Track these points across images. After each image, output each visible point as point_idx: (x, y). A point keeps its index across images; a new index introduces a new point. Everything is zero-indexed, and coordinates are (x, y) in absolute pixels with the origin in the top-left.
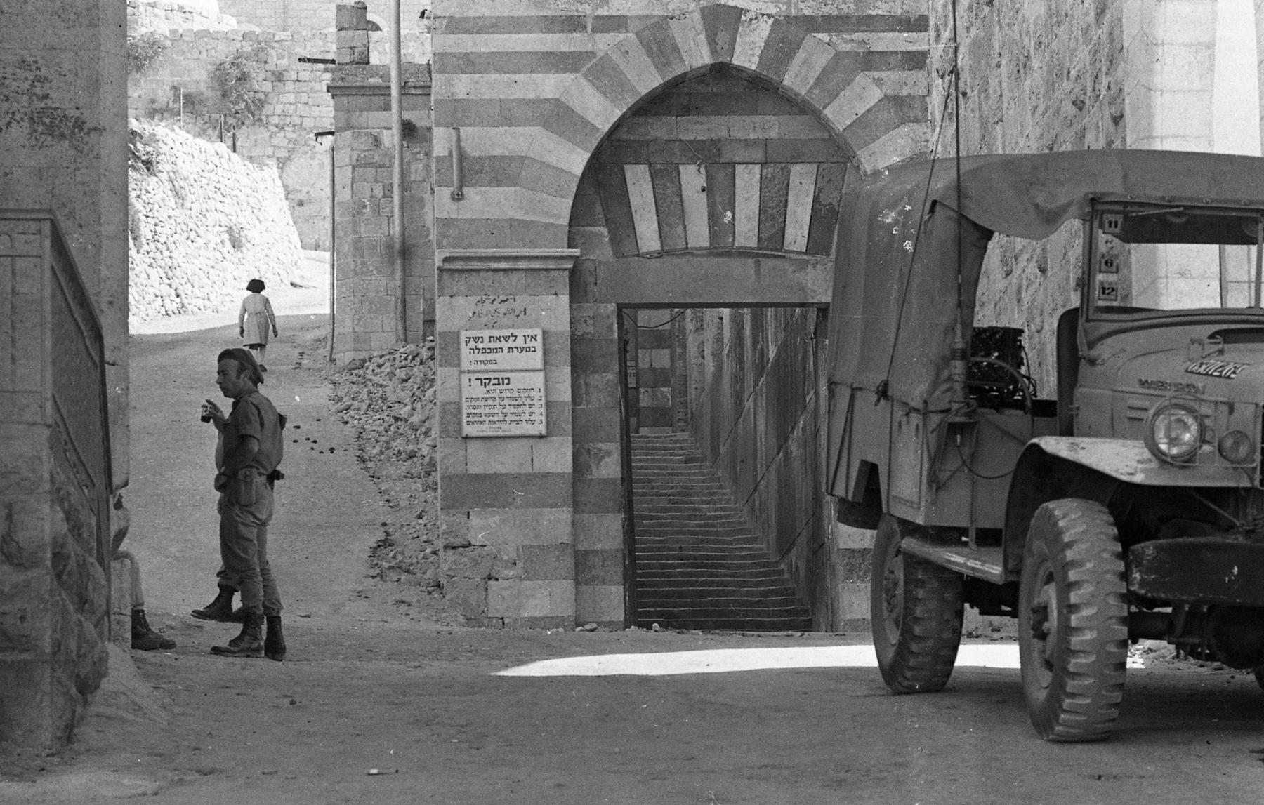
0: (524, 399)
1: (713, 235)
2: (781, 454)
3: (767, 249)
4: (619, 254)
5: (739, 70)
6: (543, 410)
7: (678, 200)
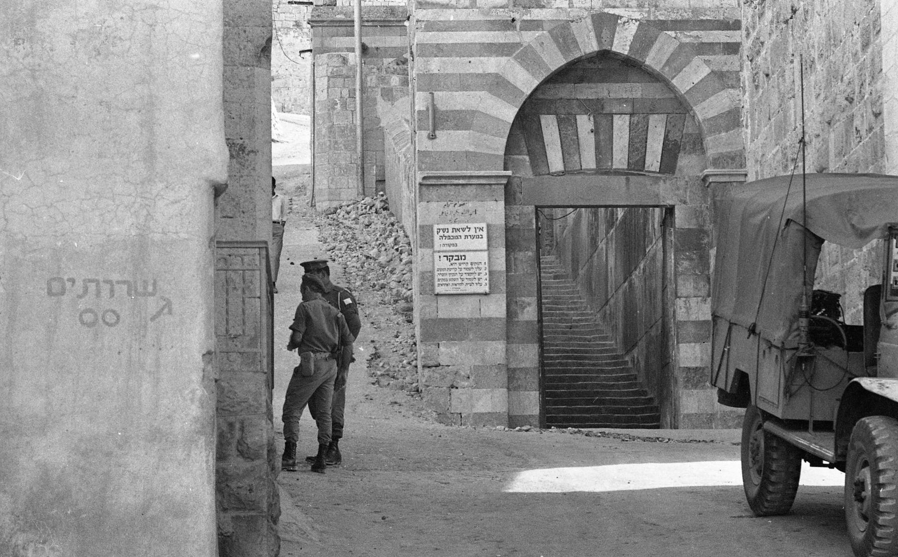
0: (475, 269)
1: (598, 161)
2: (626, 284)
3: (634, 170)
4: (537, 174)
5: (616, 54)
6: (487, 276)
7: (576, 138)
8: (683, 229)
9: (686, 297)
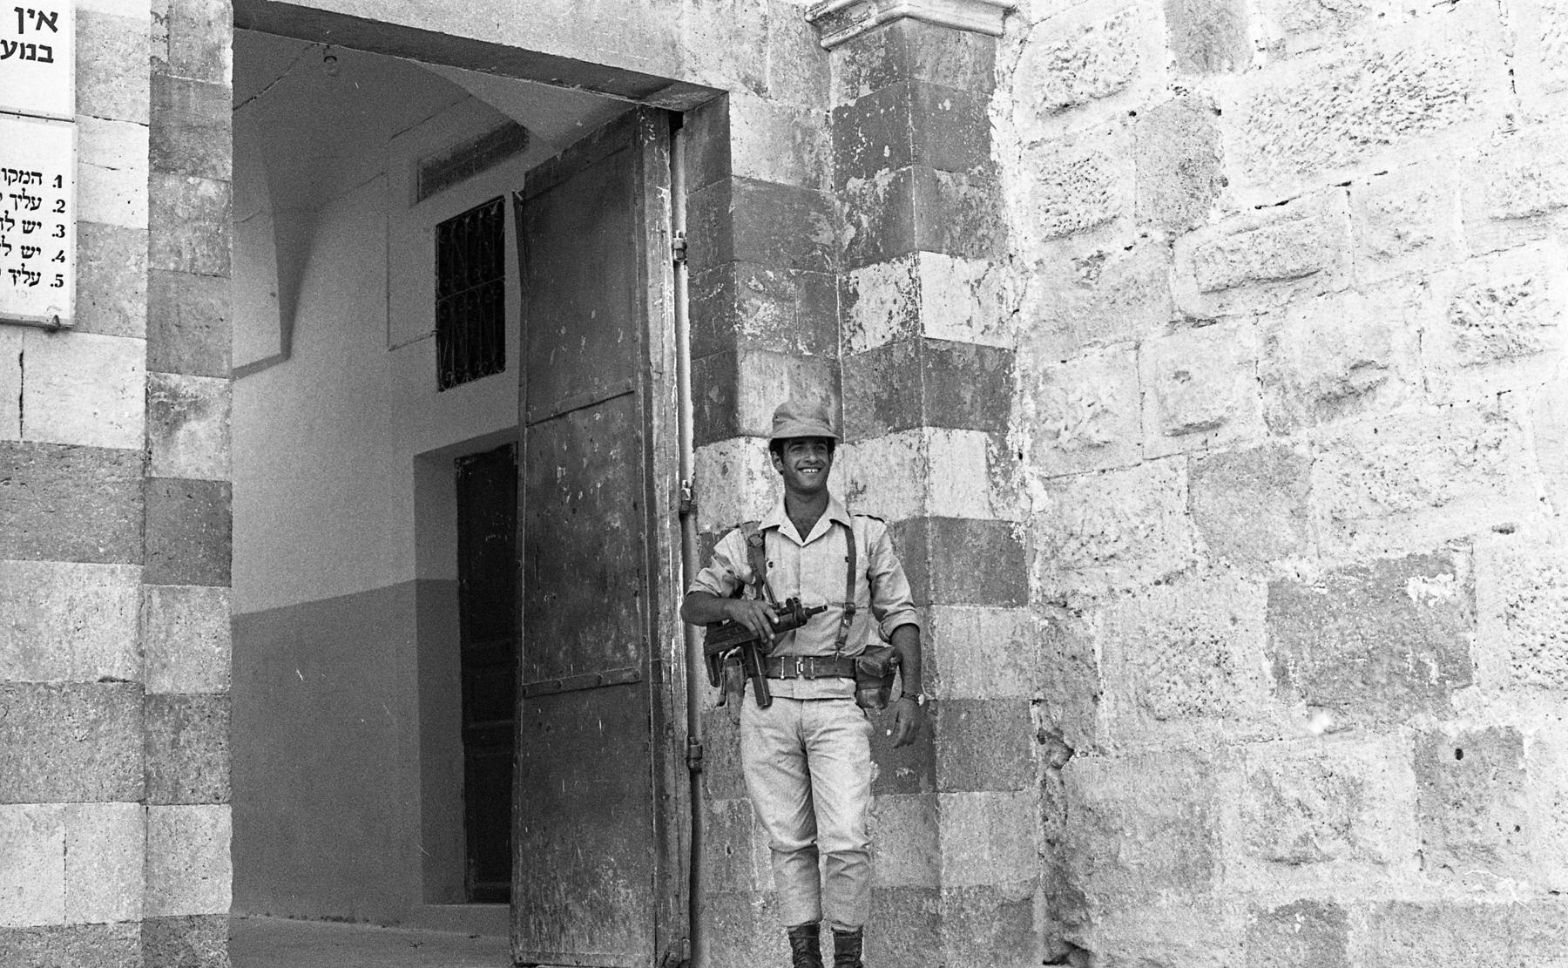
6: (68, 244)
8: (755, 182)
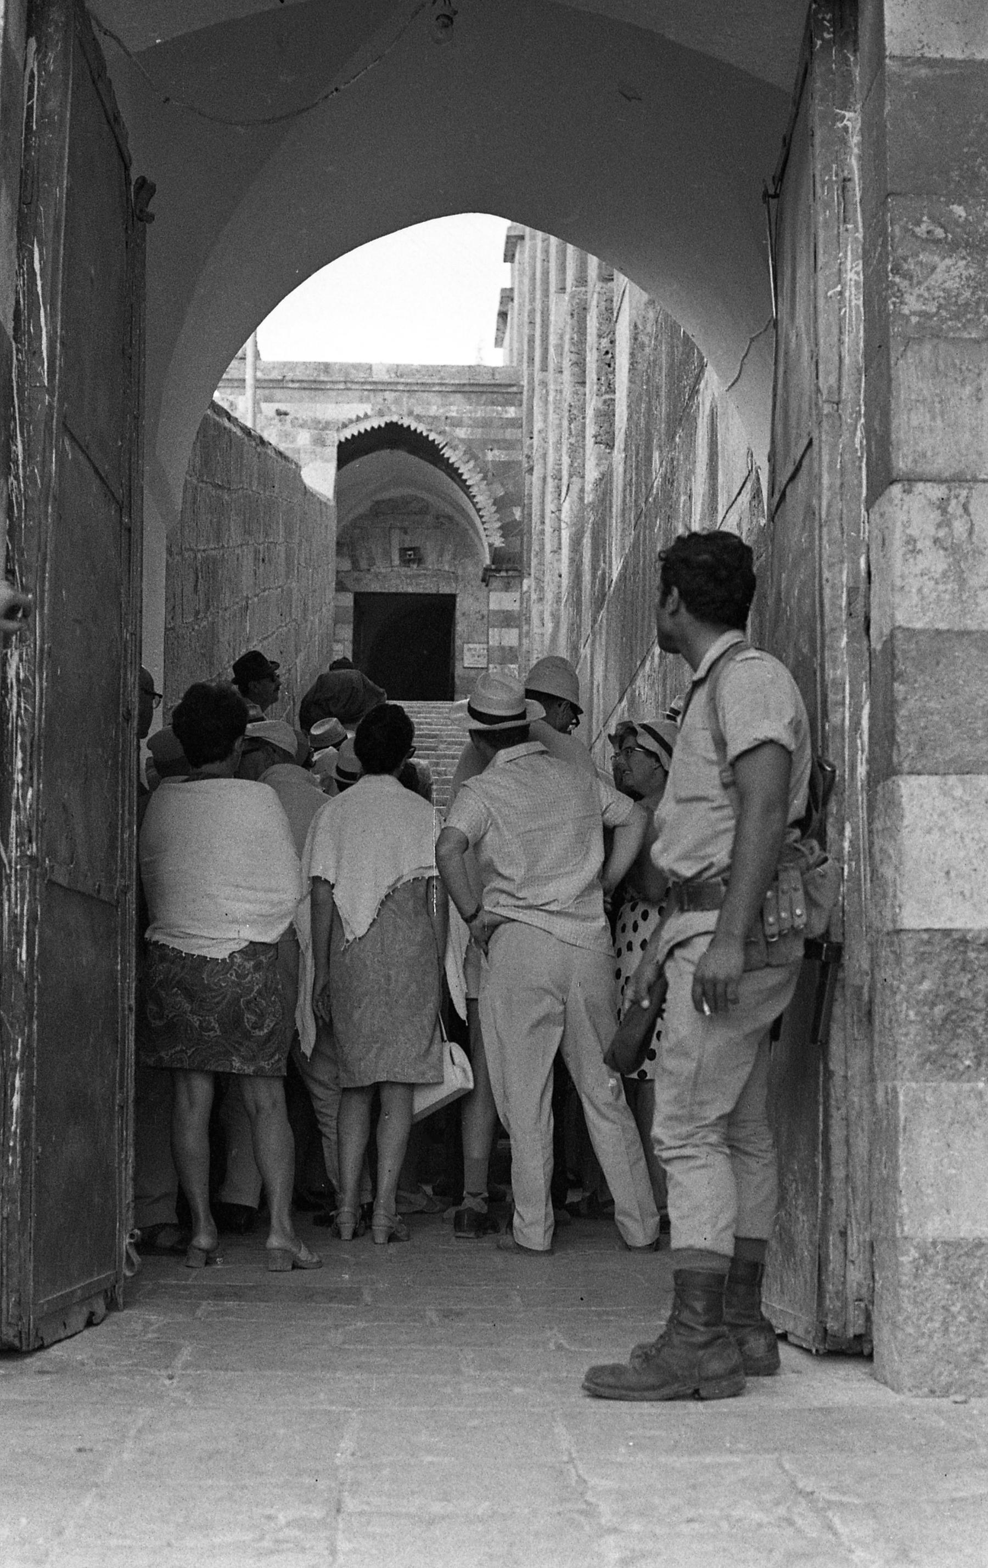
8: (931, 63)
9: (957, 479)
